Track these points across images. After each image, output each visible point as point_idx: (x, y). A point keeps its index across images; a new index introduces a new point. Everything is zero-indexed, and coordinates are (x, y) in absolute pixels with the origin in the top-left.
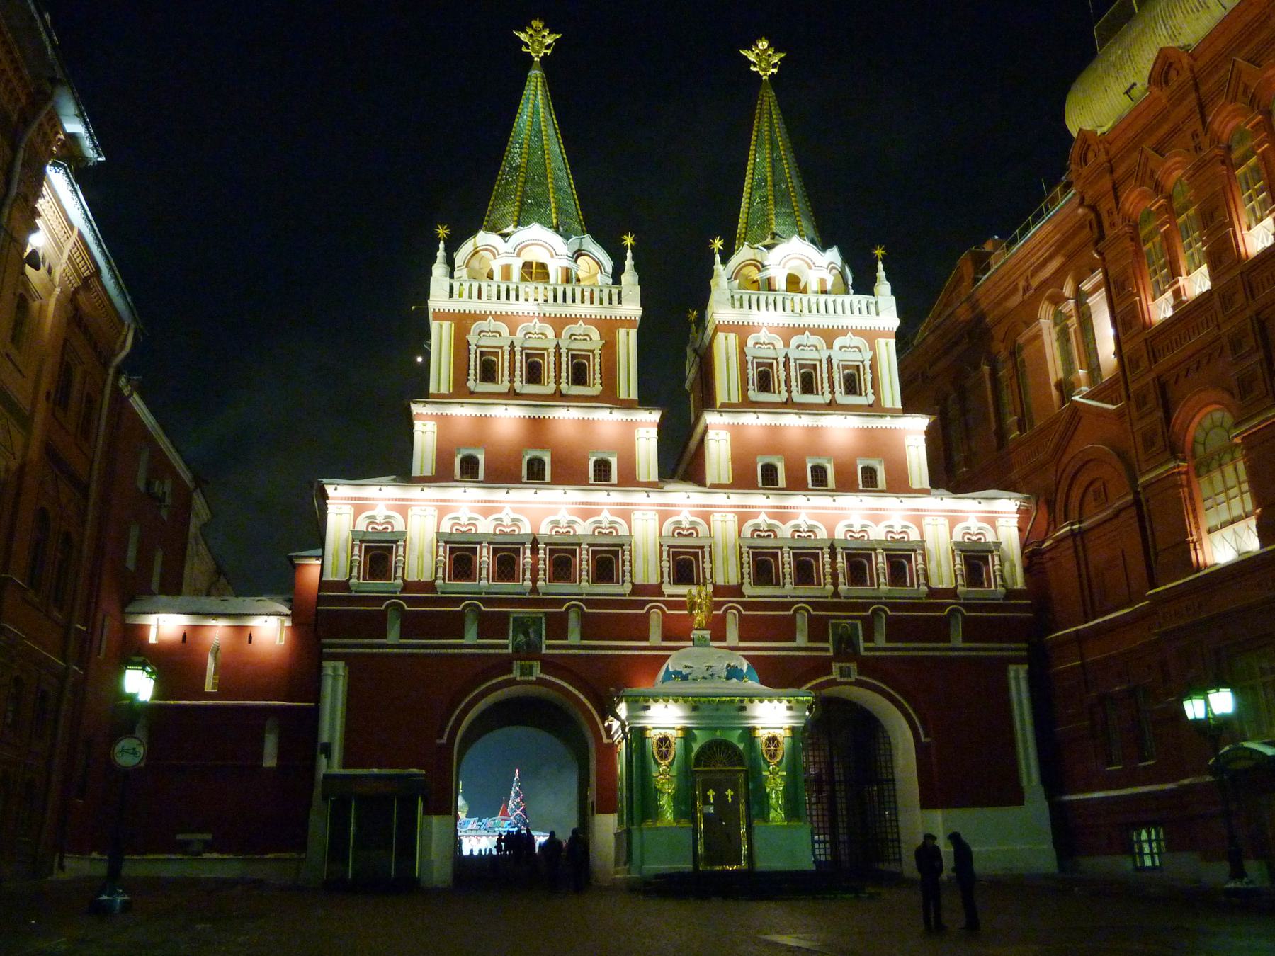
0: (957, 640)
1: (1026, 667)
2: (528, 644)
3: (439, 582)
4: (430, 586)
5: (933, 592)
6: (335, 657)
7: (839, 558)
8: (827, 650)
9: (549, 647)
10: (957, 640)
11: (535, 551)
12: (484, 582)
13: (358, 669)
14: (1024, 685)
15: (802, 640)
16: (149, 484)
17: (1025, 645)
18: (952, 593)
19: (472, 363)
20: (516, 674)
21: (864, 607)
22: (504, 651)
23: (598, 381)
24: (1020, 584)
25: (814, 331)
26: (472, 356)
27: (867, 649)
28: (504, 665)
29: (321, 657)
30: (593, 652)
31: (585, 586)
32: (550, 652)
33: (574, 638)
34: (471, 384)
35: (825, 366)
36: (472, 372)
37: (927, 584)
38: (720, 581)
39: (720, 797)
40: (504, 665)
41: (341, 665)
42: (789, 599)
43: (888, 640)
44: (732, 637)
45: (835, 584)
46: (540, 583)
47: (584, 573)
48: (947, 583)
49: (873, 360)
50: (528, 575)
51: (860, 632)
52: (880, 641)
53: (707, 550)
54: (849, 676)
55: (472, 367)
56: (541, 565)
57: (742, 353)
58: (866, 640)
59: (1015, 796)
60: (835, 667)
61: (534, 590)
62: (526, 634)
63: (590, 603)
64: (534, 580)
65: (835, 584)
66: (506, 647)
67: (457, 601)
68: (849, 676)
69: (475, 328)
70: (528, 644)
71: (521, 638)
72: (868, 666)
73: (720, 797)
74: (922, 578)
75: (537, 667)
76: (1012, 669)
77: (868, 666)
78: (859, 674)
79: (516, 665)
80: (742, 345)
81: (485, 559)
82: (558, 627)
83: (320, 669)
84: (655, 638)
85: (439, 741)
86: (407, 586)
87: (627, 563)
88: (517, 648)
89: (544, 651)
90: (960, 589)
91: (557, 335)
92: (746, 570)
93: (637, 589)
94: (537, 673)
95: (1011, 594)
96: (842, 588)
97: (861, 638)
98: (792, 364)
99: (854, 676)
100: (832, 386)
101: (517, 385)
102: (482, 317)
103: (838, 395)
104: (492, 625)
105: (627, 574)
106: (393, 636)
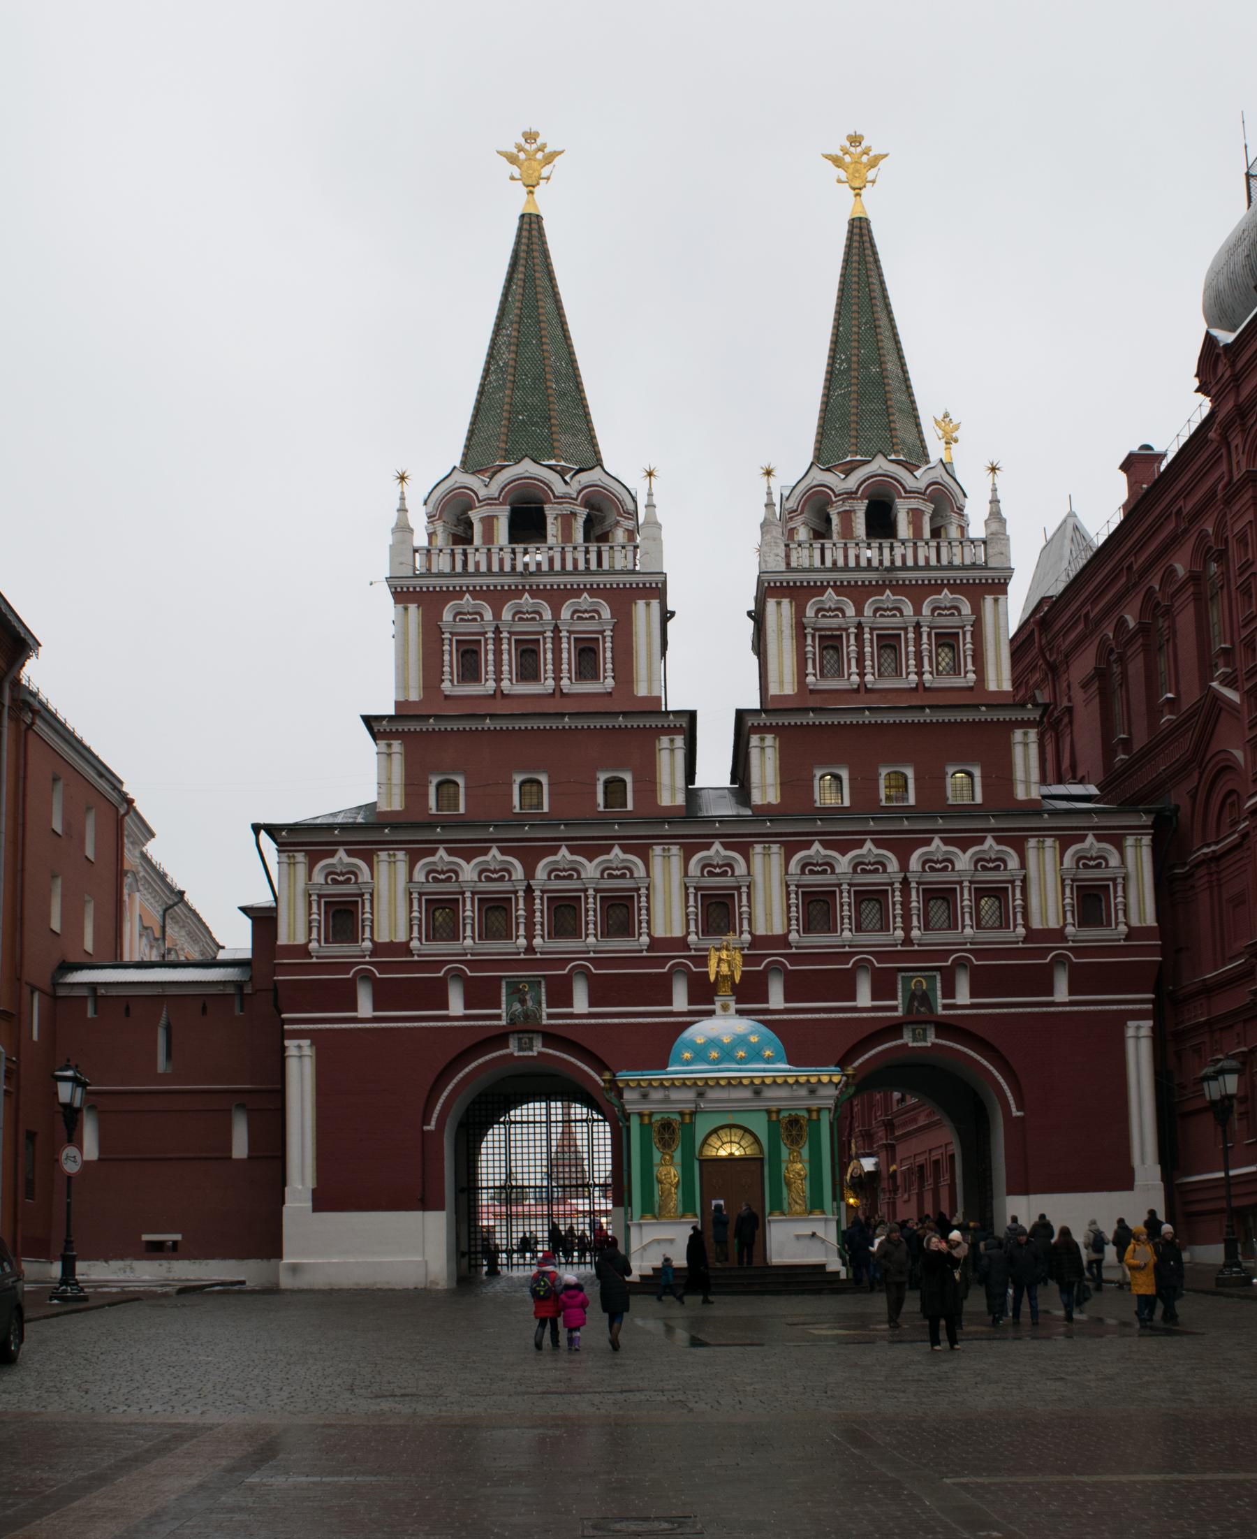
0: (1061, 993)
1: (1150, 1023)
2: (526, 1016)
3: (415, 944)
4: (404, 948)
5: (1031, 934)
7: (914, 897)
8: (895, 1009)
9: (550, 1016)
10: (1061, 993)
12: (468, 942)
13: (327, 1047)
14: (1145, 1047)
15: (864, 998)
17: (1152, 996)
18: (1059, 935)
19: (446, 657)
20: (513, 1049)
21: (945, 954)
22: (496, 1023)
23: (609, 673)
24: (1150, 920)
26: (446, 648)
27: (945, 1007)
28: (499, 1039)
29: (284, 1035)
30: (609, 1021)
32: (553, 1022)
33: (581, 1003)
34: (446, 685)
35: (911, 635)
36: (446, 669)
37: (1026, 926)
38: (761, 931)
41: (306, 1043)
42: (847, 949)
43: (972, 996)
44: (776, 999)
45: (907, 928)
46: (537, 941)
47: (591, 926)
48: (1053, 924)
49: (978, 624)
50: (522, 931)
51: (939, 985)
52: (963, 996)
53: (744, 889)
54: (925, 1041)
55: (447, 663)
56: (538, 919)
57: (800, 628)
58: (944, 997)
61: (530, 949)
62: (523, 1002)
63: (597, 962)
64: (530, 936)
65: (907, 928)
66: (498, 1017)
68: (925, 1041)
70: (526, 1016)
71: (517, 1007)
74: (1019, 916)
76: (1132, 1025)
77: (945, 1028)
78: (937, 1037)
80: (800, 613)
81: (468, 913)
82: (560, 994)
83: (284, 1049)
84: (680, 1002)
85: (426, 1128)
86: (378, 949)
87: (644, 912)
88: (512, 1019)
89: (545, 1022)
90: (1070, 930)
92: (794, 914)
93: (655, 943)
94: (538, 1047)
95: (1133, 933)
96: (915, 933)
97: (939, 993)
98: (867, 636)
99: (931, 1039)
100: (919, 664)
101: (505, 684)
103: (927, 677)
104: (480, 993)
105: (644, 925)
106: (365, 1008)
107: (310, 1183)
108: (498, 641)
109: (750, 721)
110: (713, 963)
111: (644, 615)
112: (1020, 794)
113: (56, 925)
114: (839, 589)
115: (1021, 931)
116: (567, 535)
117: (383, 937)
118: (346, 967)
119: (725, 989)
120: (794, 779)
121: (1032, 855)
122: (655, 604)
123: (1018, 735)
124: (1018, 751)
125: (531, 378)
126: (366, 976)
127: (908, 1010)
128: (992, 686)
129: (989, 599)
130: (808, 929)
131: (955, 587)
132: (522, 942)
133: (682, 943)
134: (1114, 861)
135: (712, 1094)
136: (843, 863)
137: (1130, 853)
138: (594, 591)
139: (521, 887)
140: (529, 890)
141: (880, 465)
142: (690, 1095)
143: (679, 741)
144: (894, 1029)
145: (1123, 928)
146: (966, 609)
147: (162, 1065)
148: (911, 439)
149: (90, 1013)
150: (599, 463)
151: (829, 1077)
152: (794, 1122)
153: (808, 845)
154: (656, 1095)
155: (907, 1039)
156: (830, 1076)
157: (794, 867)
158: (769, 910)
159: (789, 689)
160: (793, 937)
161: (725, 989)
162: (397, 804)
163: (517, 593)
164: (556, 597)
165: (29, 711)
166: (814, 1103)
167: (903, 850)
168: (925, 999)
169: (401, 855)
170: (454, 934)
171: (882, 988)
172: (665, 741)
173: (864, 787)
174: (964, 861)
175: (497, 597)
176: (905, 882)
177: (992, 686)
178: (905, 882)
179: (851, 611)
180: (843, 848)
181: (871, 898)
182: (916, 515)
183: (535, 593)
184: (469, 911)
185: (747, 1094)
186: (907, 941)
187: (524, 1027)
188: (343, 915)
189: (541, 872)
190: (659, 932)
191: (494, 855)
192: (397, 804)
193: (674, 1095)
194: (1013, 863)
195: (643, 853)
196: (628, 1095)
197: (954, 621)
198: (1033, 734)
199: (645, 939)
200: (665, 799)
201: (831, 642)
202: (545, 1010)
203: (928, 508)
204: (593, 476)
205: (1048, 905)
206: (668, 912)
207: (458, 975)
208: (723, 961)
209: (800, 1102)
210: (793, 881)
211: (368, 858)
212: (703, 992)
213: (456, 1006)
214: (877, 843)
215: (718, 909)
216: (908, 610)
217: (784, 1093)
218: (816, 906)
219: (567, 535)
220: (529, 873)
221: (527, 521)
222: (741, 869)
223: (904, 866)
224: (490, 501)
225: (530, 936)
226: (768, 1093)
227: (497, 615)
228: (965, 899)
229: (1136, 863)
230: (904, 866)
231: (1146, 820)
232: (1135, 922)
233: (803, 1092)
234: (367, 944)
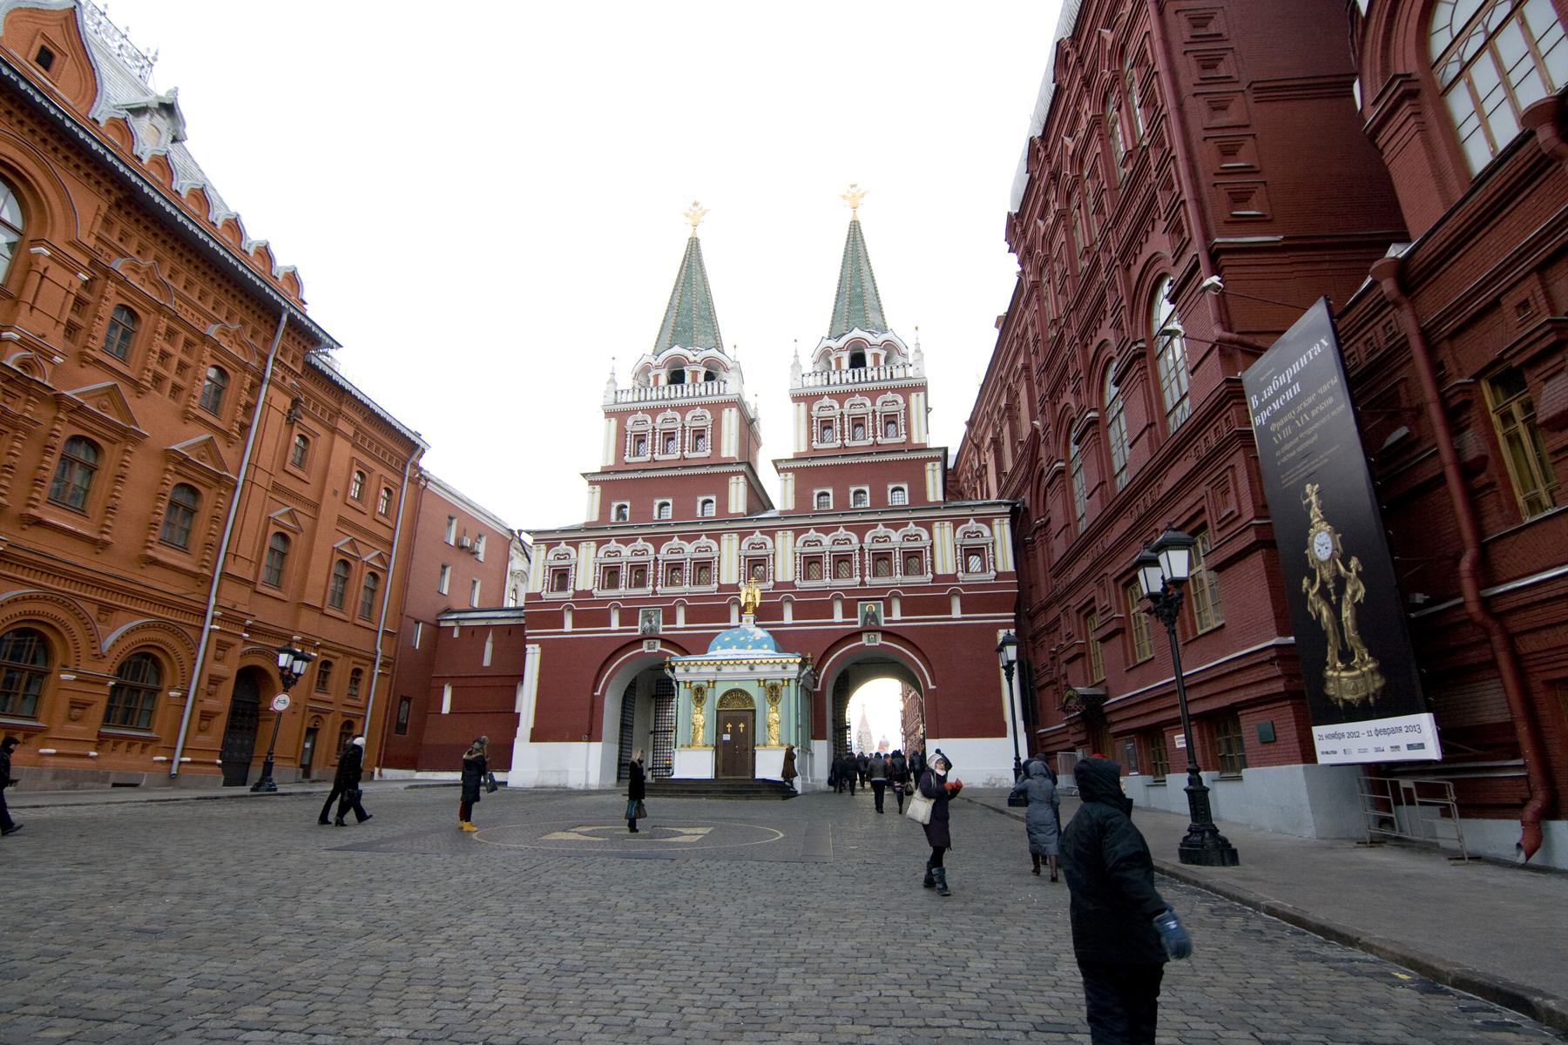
0: (956, 612)
4: (589, 593)
5: (936, 578)
6: (533, 642)
10: (956, 612)
11: (656, 565)
15: (838, 616)
16: (457, 540)
18: (954, 577)
20: (645, 648)
24: (1011, 567)
25: (863, 393)
28: (638, 642)
29: (526, 642)
31: (687, 588)
33: (681, 622)
34: (627, 458)
39: (735, 728)
40: (638, 642)
45: (862, 576)
46: (658, 588)
48: (951, 571)
49: (907, 408)
57: (810, 417)
59: (1000, 732)
60: (865, 637)
61: (654, 592)
63: (690, 598)
64: (655, 585)
65: (862, 576)
67: (604, 602)
69: (630, 422)
72: (887, 634)
73: (735, 728)
75: (658, 643)
77: (887, 634)
79: (645, 643)
80: (809, 409)
82: (670, 617)
84: (734, 621)
86: (577, 594)
90: (960, 574)
91: (683, 419)
93: (721, 587)
95: (999, 576)
96: (867, 579)
101: (656, 456)
102: (635, 412)
104: (628, 617)
106: (568, 625)
107: (531, 725)
108: (654, 434)
109: (780, 466)
110: (743, 594)
111: (730, 419)
112: (931, 498)
113: (445, 592)
114: (831, 395)
115: (930, 576)
116: (694, 379)
117: (579, 588)
118: (559, 604)
119: (750, 610)
120: (802, 495)
121: (936, 531)
122: (734, 410)
123: (929, 466)
124: (929, 475)
125: (691, 311)
126: (570, 609)
127: (865, 623)
128: (915, 441)
129: (914, 395)
130: (807, 577)
131: (894, 390)
132: (650, 588)
133: (736, 588)
134: (986, 532)
135: (725, 669)
136: (827, 540)
137: (996, 528)
138: (703, 406)
139: (652, 558)
140: (656, 560)
141: (857, 333)
142: (713, 669)
143: (742, 478)
144: (857, 635)
145: (993, 573)
146: (901, 400)
147: (487, 662)
148: (878, 322)
149: (456, 634)
150: (718, 346)
151: (794, 660)
152: (774, 687)
153: (807, 531)
154: (693, 670)
155: (865, 640)
156: (794, 660)
157: (800, 542)
158: (785, 568)
159: (803, 449)
160: (797, 582)
161: (750, 610)
162: (595, 518)
163: (664, 409)
164: (683, 410)
165: (420, 481)
166: (786, 676)
167: (861, 530)
168: (874, 617)
169: (593, 544)
170: (613, 584)
171: (849, 611)
172: (734, 479)
173: (841, 501)
174: (896, 537)
175: (654, 412)
176: (862, 549)
177: (915, 441)
178: (862, 549)
179: (837, 406)
180: (826, 531)
181: (842, 559)
182: (876, 356)
183: (673, 408)
184: (624, 573)
185: (746, 669)
186: (862, 583)
187: (650, 636)
188: (561, 576)
189: (664, 550)
190: (724, 581)
191: (640, 544)
192: (595, 518)
193: (704, 669)
194: (925, 535)
195: (716, 537)
196: (677, 670)
197: (894, 408)
198: (938, 465)
199: (716, 585)
200: (732, 510)
201: (827, 425)
202: (661, 626)
203: (883, 354)
204: (713, 352)
205: (946, 561)
206: (729, 571)
207: (617, 607)
208: (751, 594)
209: (776, 674)
210: (798, 550)
211: (576, 545)
212: (742, 610)
213: (615, 624)
214: (847, 528)
215: (756, 565)
216: (868, 402)
217: (767, 668)
218: (811, 562)
219: (694, 379)
220: (657, 551)
221: (677, 377)
222: (769, 543)
223: (861, 540)
224: (657, 367)
225: (655, 585)
226: (758, 669)
227: (654, 421)
228: (897, 559)
229: (1001, 534)
230: (861, 540)
231: (1008, 509)
232: (1000, 569)
233: (779, 668)
234: (571, 592)
